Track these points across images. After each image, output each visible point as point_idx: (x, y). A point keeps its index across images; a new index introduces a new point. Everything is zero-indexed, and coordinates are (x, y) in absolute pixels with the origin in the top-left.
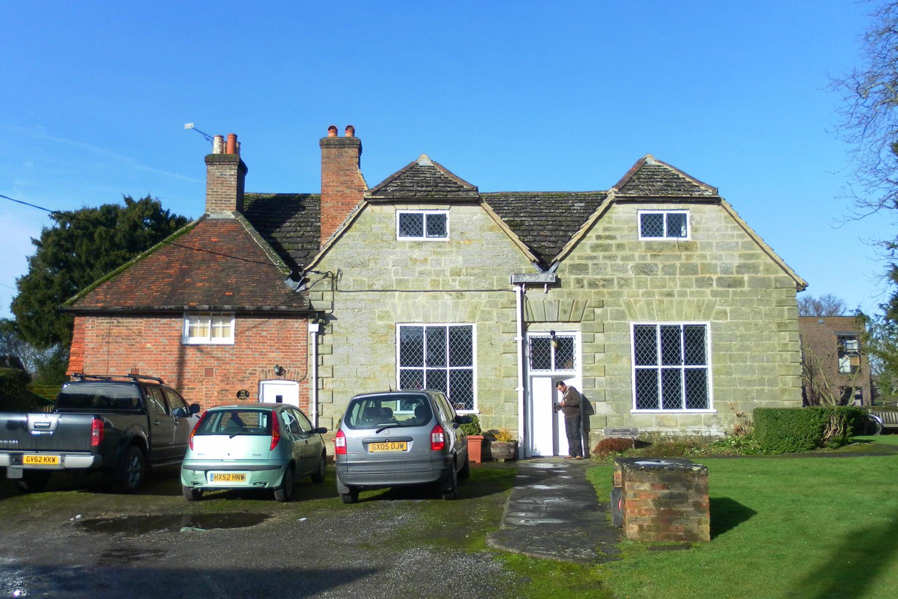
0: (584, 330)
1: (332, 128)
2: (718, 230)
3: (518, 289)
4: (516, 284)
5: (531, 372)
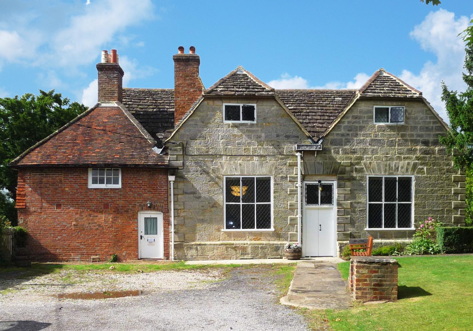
0: (339, 179)
1: (181, 49)
2: (421, 119)
3: (298, 154)
4: (297, 151)
5: (306, 206)
